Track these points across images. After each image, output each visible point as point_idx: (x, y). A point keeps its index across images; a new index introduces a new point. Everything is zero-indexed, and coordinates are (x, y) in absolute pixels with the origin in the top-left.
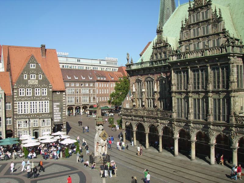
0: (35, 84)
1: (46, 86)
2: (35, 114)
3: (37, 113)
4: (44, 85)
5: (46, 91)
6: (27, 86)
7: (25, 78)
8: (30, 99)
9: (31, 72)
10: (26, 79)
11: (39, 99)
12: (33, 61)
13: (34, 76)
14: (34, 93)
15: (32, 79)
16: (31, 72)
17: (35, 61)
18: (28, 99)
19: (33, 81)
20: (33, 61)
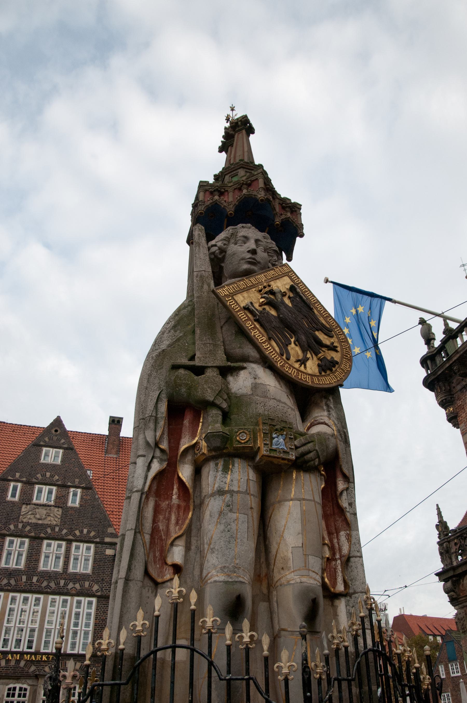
0: (46, 522)
1: (92, 534)
2: (22, 654)
3: (33, 650)
4: (85, 531)
5: (83, 559)
6: (12, 527)
7: (13, 495)
8: (13, 582)
9: (39, 476)
10: (17, 499)
11: (52, 585)
12: (55, 438)
13: (50, 492)
14: (38, 560)
15: (38, 502)
16: (39, 476)
17: (63, 441)
18: (5, 581)
19: (43, 512)
20: (55, 438)
